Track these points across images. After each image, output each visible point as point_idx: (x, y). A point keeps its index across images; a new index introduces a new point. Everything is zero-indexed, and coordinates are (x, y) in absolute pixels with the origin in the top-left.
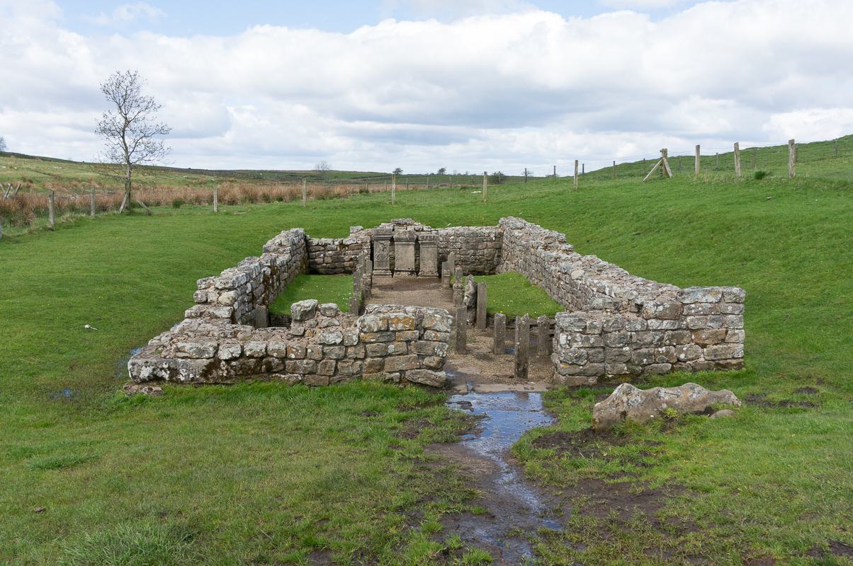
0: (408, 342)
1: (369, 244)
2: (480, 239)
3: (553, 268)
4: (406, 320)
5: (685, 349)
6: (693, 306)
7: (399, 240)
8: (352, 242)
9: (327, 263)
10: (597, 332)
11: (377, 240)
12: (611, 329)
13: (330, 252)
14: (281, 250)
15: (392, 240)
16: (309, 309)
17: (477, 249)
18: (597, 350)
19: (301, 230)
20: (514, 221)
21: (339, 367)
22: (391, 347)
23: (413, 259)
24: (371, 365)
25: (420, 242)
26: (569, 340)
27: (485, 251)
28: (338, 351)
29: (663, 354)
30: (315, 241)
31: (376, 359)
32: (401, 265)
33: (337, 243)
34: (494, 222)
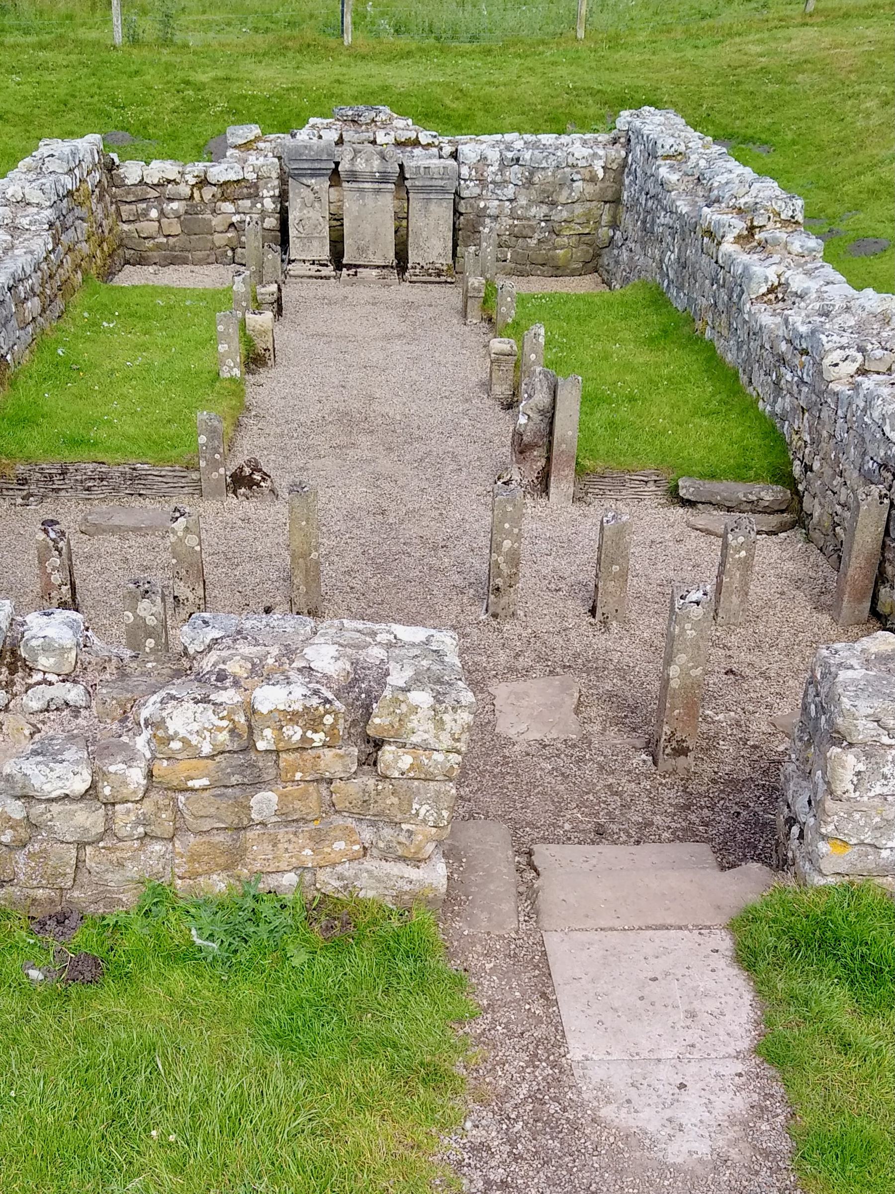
13: (175, 205)
17: (553, 204)
20: (657, 124)
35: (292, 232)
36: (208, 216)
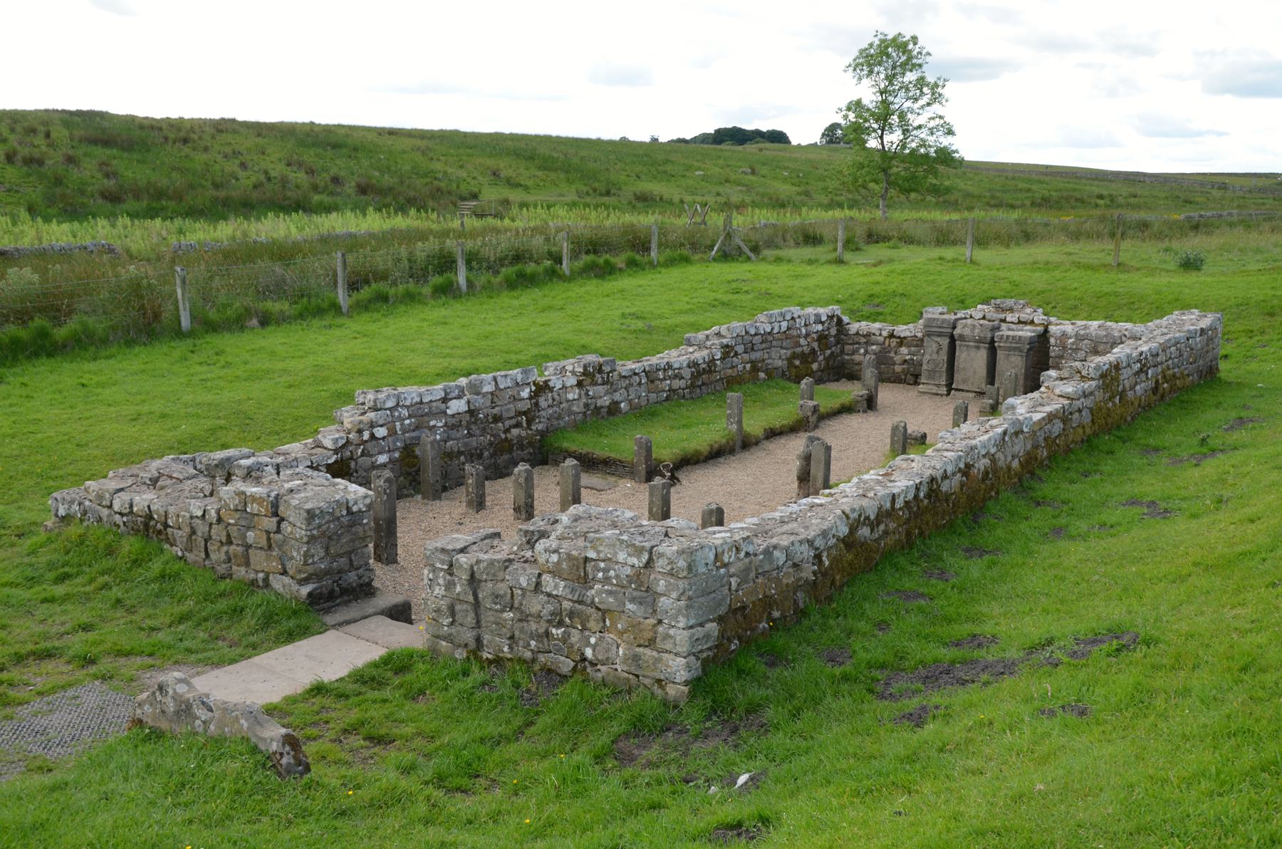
5: (593, 640)
6: (602, 565)
7: (962, 337)
8: (908, 334)
29: (558, 639)
30: (854, 327)
32: (964, 381)
33: (885, 333)
36: (892, 354)
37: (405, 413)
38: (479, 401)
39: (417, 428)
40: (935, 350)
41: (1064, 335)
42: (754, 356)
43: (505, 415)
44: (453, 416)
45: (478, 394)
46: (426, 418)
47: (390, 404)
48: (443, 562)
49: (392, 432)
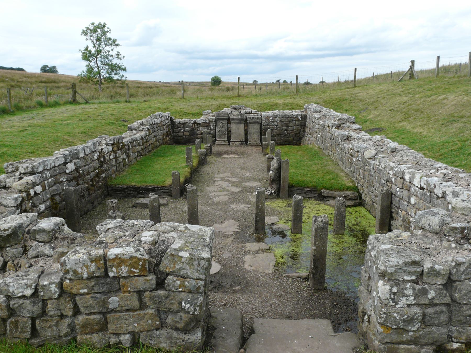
0: (140, 293)
1: (214, 122)
2: (290, 119)
3: (346, 145)
4: (133, 262)
7: (233, 120)
8: (203, 121)
9: (186, 136)
10: (440, 281)
11: (218, 120)
12: (463, 277)
13: (188, 128)
14: (142, 127)
15: (229, 120)
16: (7, 233)
17: (288, 126)
18: (438, 308)
19: (167, 114)
21: (38, 328)
22: (114, 301)
23: (243, 133)
24: (85, 325)
25: (248, 121)
26: (394, 294)
27: (294, 127)
28: (30, 309)
30: (178, 120)
31: (92, 317)
32: (235, 138)
33: (192, 122)
34: (300, 107)
35: (217, 134)
37: (48, 174)
38: (80, 163)
39: (55, 184)
40: (221, 126)
41: (268, 117)
42: (156, 133)
43: (90, 170)
44: (69, 174)
45: (78, 158)
46: (58, 177)
47: (40, 169)
48: (410, 274)
49: (44, 189)
